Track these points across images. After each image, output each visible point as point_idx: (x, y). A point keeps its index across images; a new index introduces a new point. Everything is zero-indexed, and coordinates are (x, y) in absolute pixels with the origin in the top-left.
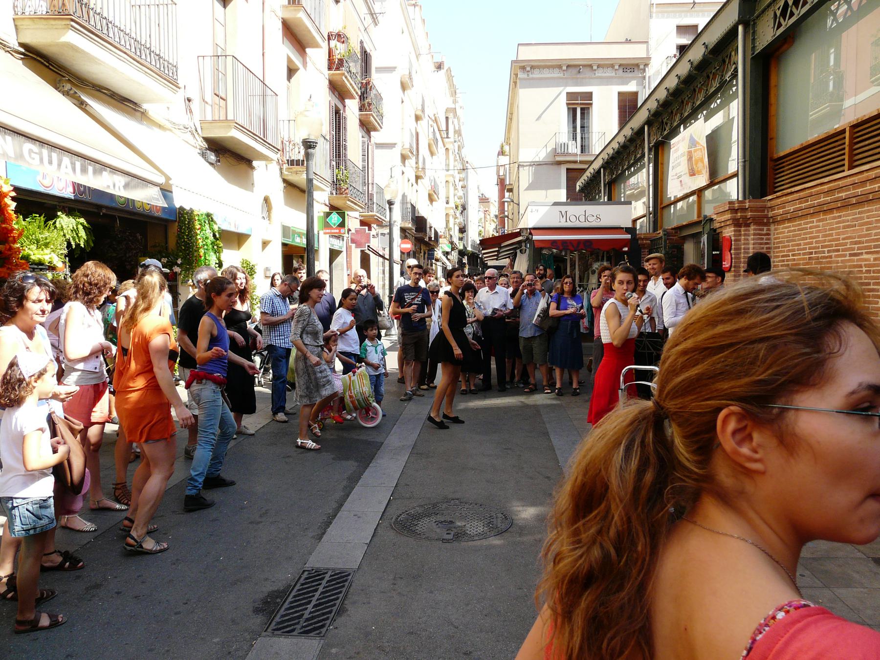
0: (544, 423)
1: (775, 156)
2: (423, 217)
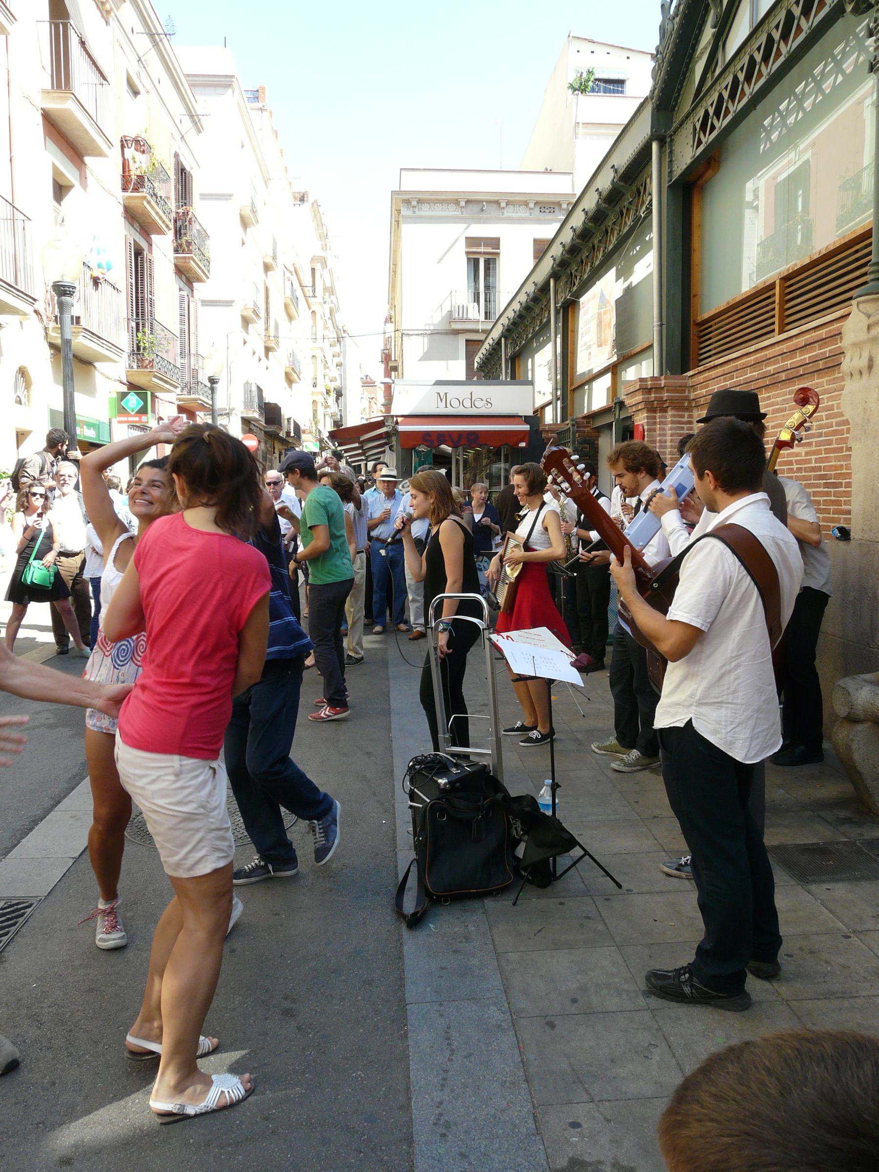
0: (388, 679)
1: (700, 319)
2: (276, 405)
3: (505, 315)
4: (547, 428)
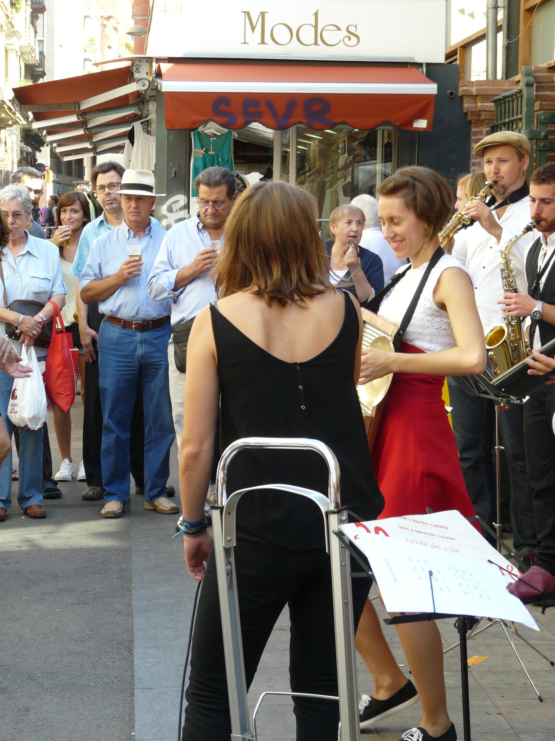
0: (130, 615)
4: (474, 90)
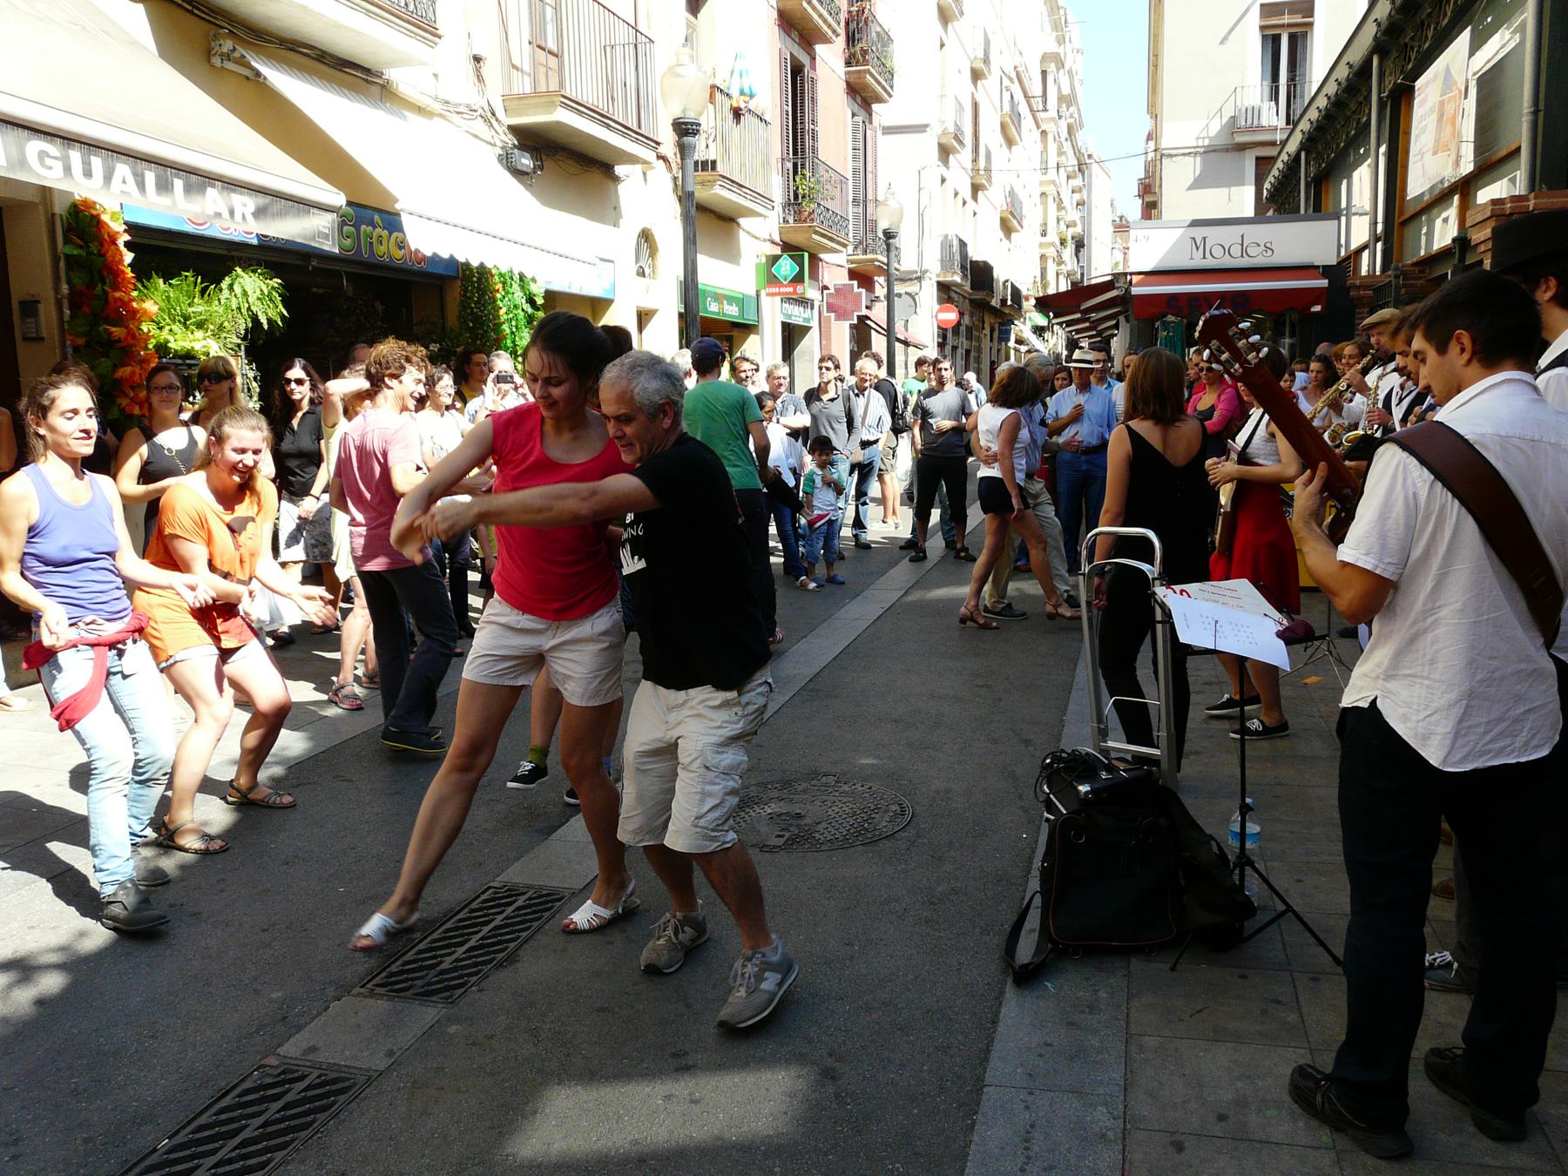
3: (1306, 117)
